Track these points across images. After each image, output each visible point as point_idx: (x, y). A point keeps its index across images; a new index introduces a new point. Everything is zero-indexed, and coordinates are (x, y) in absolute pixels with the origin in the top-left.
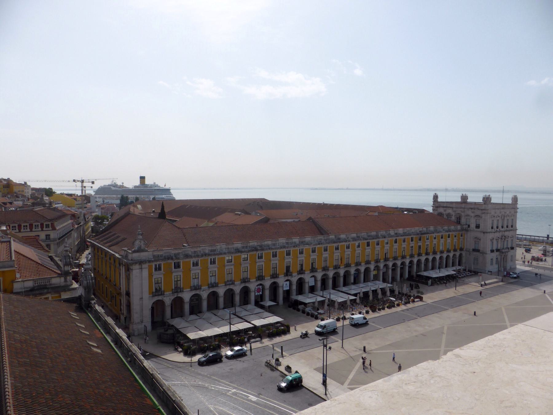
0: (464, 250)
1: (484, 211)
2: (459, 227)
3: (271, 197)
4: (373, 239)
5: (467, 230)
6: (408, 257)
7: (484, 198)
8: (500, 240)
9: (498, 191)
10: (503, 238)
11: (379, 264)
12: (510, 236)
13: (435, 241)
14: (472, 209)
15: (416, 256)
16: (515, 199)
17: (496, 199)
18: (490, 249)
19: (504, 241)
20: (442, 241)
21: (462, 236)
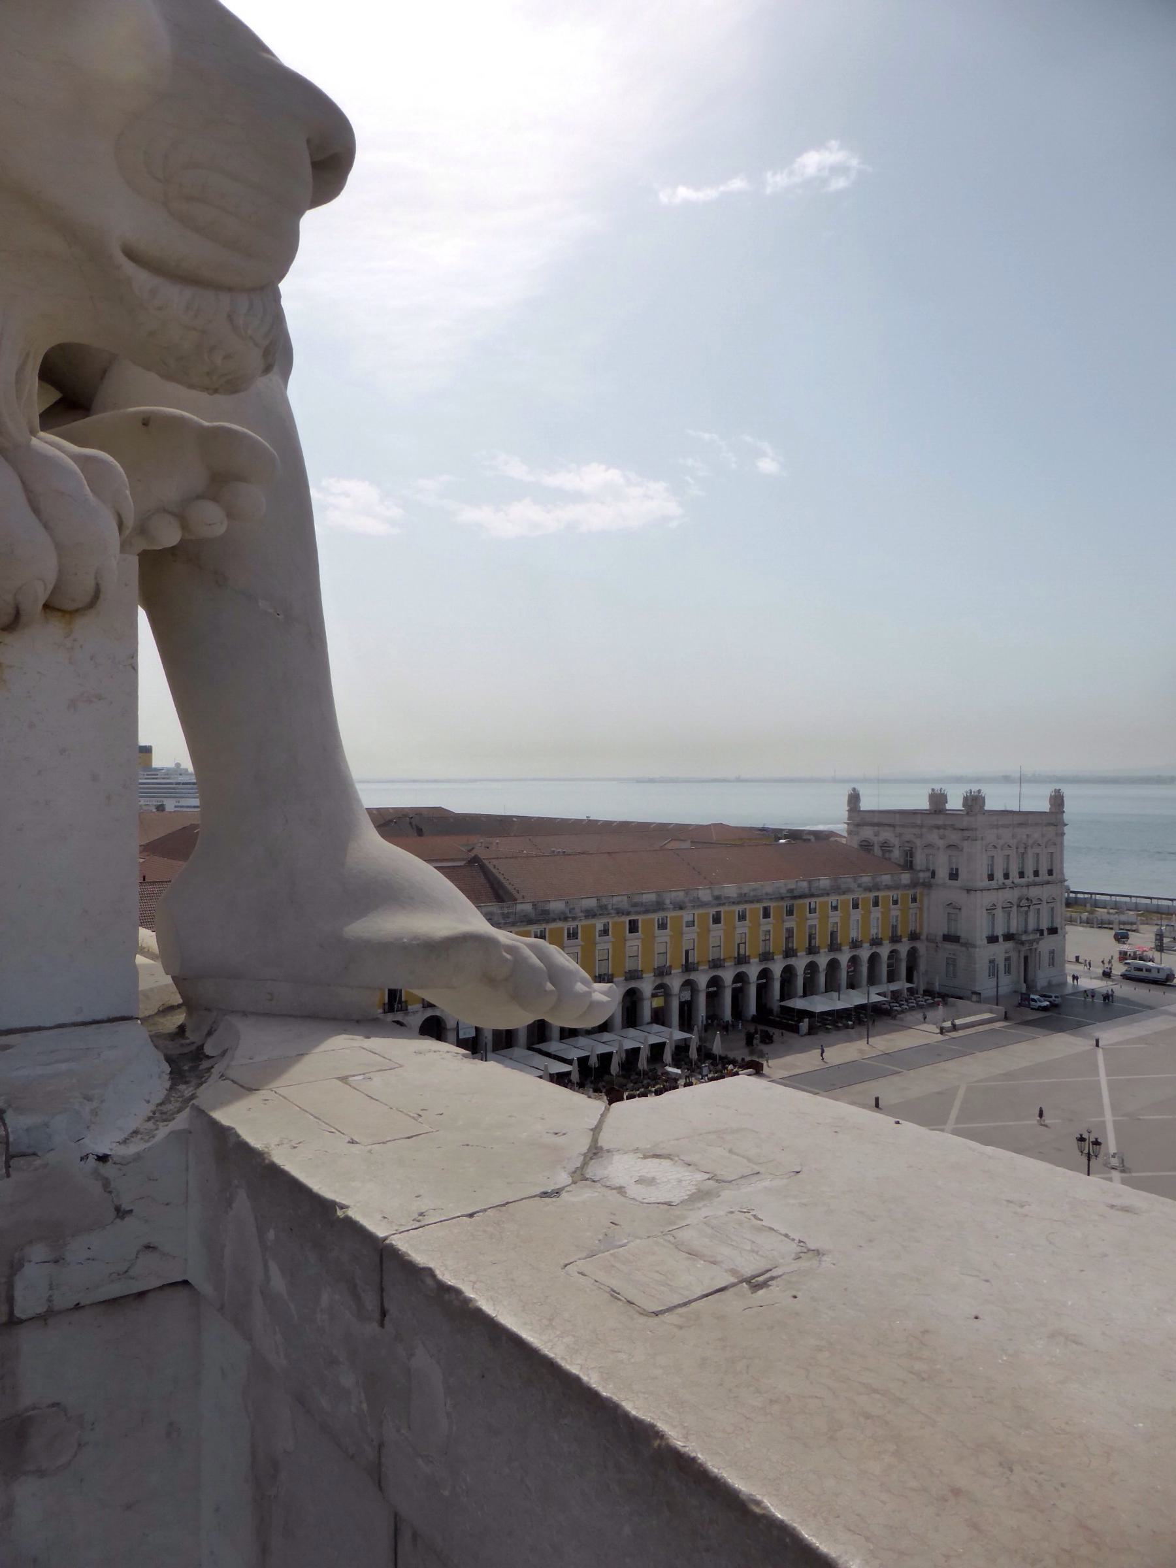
0: (923, 937)
1: (966, 834)
2: (906, 878)
3: (460, 803)
4: (647, 912)
5: (928, 886)
6: (754, 960)
7: (966, 799)
8: (1015, 909)
9: (1007, 779)
10: (1026, 904)
11: (667, 980)
12: (1044, 899)
13: (835, 917)
14: (938, 827)
15: (778, 957)
16: (1058, 800)
17: (997, 800)
18: (986, 933)
19: (1027, 913)
20: (856, 915)
21: (914, 900)
